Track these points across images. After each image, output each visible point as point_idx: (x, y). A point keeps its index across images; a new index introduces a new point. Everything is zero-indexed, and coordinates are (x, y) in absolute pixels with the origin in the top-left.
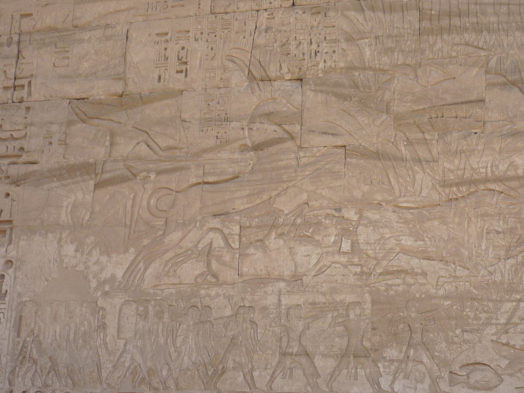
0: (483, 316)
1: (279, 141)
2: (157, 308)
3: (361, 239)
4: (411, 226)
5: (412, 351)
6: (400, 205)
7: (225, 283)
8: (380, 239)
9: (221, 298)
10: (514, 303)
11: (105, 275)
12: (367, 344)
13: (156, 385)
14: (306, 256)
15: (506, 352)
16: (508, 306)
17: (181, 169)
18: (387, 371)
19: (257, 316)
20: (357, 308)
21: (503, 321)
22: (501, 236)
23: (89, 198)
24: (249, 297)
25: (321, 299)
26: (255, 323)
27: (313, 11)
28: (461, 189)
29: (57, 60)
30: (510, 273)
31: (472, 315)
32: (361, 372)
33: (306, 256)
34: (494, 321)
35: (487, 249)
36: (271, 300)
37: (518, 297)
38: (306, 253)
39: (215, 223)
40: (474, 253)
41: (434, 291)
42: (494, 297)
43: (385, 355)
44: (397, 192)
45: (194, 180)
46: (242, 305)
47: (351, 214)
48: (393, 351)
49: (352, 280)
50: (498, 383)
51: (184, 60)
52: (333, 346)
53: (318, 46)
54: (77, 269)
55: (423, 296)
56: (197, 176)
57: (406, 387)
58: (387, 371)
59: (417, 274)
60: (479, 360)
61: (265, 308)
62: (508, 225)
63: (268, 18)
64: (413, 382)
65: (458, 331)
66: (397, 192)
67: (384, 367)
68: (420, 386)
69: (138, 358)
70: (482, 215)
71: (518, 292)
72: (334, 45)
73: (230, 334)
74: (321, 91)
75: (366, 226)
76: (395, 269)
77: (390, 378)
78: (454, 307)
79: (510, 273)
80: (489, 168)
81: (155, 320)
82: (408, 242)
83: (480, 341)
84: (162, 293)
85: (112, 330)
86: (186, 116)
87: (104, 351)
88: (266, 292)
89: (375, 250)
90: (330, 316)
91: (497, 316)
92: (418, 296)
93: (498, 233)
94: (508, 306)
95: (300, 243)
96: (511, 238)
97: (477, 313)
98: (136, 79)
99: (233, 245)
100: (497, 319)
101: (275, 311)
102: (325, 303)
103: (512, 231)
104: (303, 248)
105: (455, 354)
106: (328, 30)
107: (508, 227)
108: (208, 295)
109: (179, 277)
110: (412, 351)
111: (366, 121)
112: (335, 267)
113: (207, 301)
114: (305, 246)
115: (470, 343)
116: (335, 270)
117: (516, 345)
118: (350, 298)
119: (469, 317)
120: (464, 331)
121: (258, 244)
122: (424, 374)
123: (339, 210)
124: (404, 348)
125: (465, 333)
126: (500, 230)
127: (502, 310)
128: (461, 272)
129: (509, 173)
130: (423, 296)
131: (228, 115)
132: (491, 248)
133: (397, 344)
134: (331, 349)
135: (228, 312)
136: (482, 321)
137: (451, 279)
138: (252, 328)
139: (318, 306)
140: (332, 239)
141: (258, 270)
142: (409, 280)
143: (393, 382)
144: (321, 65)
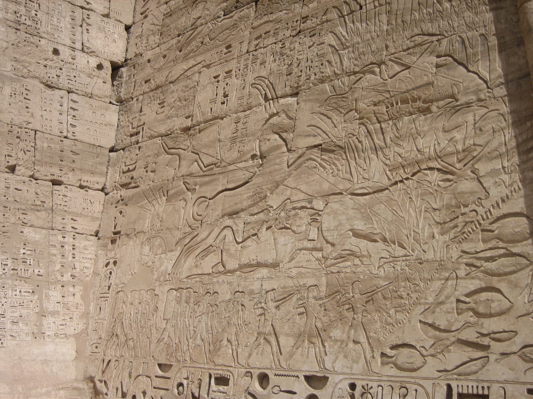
0: (414, 296)
1: (278, 147)
2: (188, 294)
3: (325, 226)
4: (363, 211)
5: (352, 332)
6: (356, 192)
7: (229, 272)
8: (338, 226)
9: (226, 285)
10: (443, 282)
11: (163, 268)
12: (319, 325)
13: (179, 358)
14: (284, 245)
15: (432, 332)
16: (438, 284)
17: (214, 180)
18: (331, 350)
19: (246, 302)
20: (315, 290)
21: (431, 300)
22: (438, 212)
23: (161, 209)
24: (243, 283)
25: (290, 283)
26: (244, 305)
27: (312, 33)
28: (406, 170)
29: (159, 109)
30: (442, 251)
31: (404, 295)
32: (312, 351)
33: (284, 245)
34: (423, 301)
35: (423, 229)
36: (256, 286)
37: (447, 275)
38: (284, 243)
39: (228, 222)
40: (412, 233)
41: (376, 272)
42: (426, 275)
43: (331, 335)
44: (355, 181)
45: (220, 188)
46: (238, 290)
47: (319, 204)
48: (338, 331)
49: (315, 264)
50: (422, 365)
51: (227, 93)
52: (294, 326)
53: (312, 62)
54: (148, 265)
55: (366, 278)
56: (223, 185)
57: (344, 367)
58: (331, 350)
59: (363, 256)
60: (407, 341)
61: (252, 292)
62: (443, 202)
63: (281, 48)
64: (350, 362)
65: (392, 311)
66: (355, 181)
67: (330, 347)
68: (355, 366)
69: (172, 335)
70: (422, 195)
71: (446, 269)
72: (322, 58)
73: (227, 315)
74: (310, 100)
75: (328, 214)
76: (347, 252)
77: (333, 357)
78: (390, 288)
79: (442, 251)
80: (432, 148)
81: (185, 305)
82: (360, 226)
83: (409, 321)
84: (191, 282)
85: (160, 313)
86: (222, 137)
87: (154, 330)
88: (254, 278)
89: (333, 236)
90: (294, 298)
91: (426, 296)
92: (362, 277)
93: (435, 210)
94: (438, 284)
95: (281, 234)
96: (446, 215)
97: (410, 293)
98: (198, 114)
99: (237, 240)
100: (426, 299)
101: (258, 295)
102: (292, 287)
103: (448, 207)
104: (283, 238)
105: (387, 334)
106: (319, 47)
107: (444, 203)
108: (218, 282)
109: (202, 269)
110: (352, 332)
111: (338, 119)
112: (303, 254)
113: (217, 288)
114: (284, 236)
115: (400, 324)
116: (302, 256)
117: (440, 326)
118: (311, 281)
119: (401, 297)
120: (396, 312)
121: (254, 237)
122: (360, 354)
123: (310, 202)
124: (347, 328)
125: (397, 314)
126: (435, 207)
127: (431, 289)
128: (400, 252)
129: (449, 149)
130: (366, 278)
131: (248, 131)
132: (427, 227)
133: (342, 324)
134: (293, 329)
135: (228, 297)
136: (413, 300)
137: (391, 259)
138: (242, 310)
139: (288, 290)
140: (304, 228)
141: (251, 260)
142: (357, 261)
143: (335, 361)
144: (312, 78)
